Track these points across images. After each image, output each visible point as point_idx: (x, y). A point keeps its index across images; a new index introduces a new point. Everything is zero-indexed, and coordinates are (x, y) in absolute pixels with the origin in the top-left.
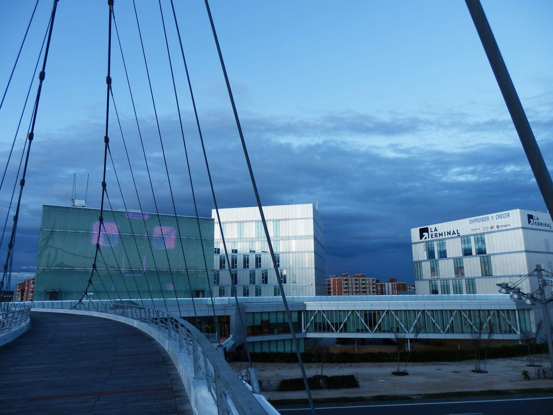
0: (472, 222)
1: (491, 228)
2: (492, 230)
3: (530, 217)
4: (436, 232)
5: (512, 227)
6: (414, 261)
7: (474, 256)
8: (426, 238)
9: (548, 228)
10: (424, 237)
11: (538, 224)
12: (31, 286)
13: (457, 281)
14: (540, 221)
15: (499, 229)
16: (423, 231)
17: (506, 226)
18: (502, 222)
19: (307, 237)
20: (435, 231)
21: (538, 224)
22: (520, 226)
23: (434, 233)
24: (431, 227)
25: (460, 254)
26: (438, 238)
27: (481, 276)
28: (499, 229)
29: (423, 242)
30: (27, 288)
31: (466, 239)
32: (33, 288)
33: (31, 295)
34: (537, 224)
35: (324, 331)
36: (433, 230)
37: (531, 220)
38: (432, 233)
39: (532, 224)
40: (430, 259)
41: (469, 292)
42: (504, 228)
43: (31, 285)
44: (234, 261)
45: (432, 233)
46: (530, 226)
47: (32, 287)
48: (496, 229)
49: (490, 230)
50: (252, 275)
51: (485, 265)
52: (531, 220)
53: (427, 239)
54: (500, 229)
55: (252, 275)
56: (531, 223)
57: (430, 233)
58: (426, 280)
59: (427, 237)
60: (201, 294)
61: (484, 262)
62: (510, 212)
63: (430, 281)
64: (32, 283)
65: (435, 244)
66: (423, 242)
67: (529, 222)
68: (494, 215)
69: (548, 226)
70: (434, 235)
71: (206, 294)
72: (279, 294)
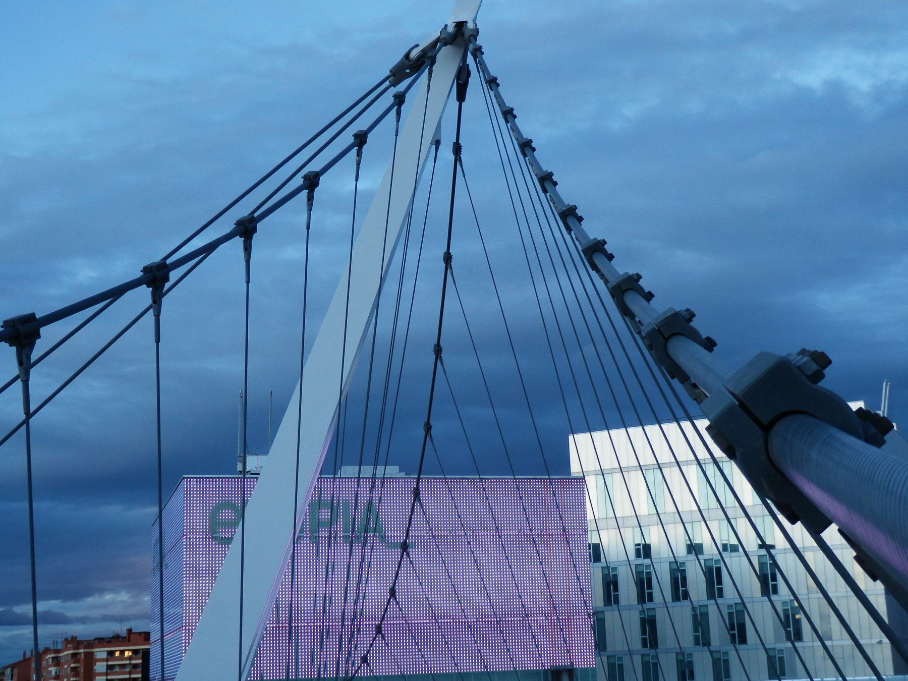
12: (51, 671)
43: (50, 669)
44: (644, 583)
47: (53, 673)
50: (700, 621)
55: (700, 621)
64: (53, 661)
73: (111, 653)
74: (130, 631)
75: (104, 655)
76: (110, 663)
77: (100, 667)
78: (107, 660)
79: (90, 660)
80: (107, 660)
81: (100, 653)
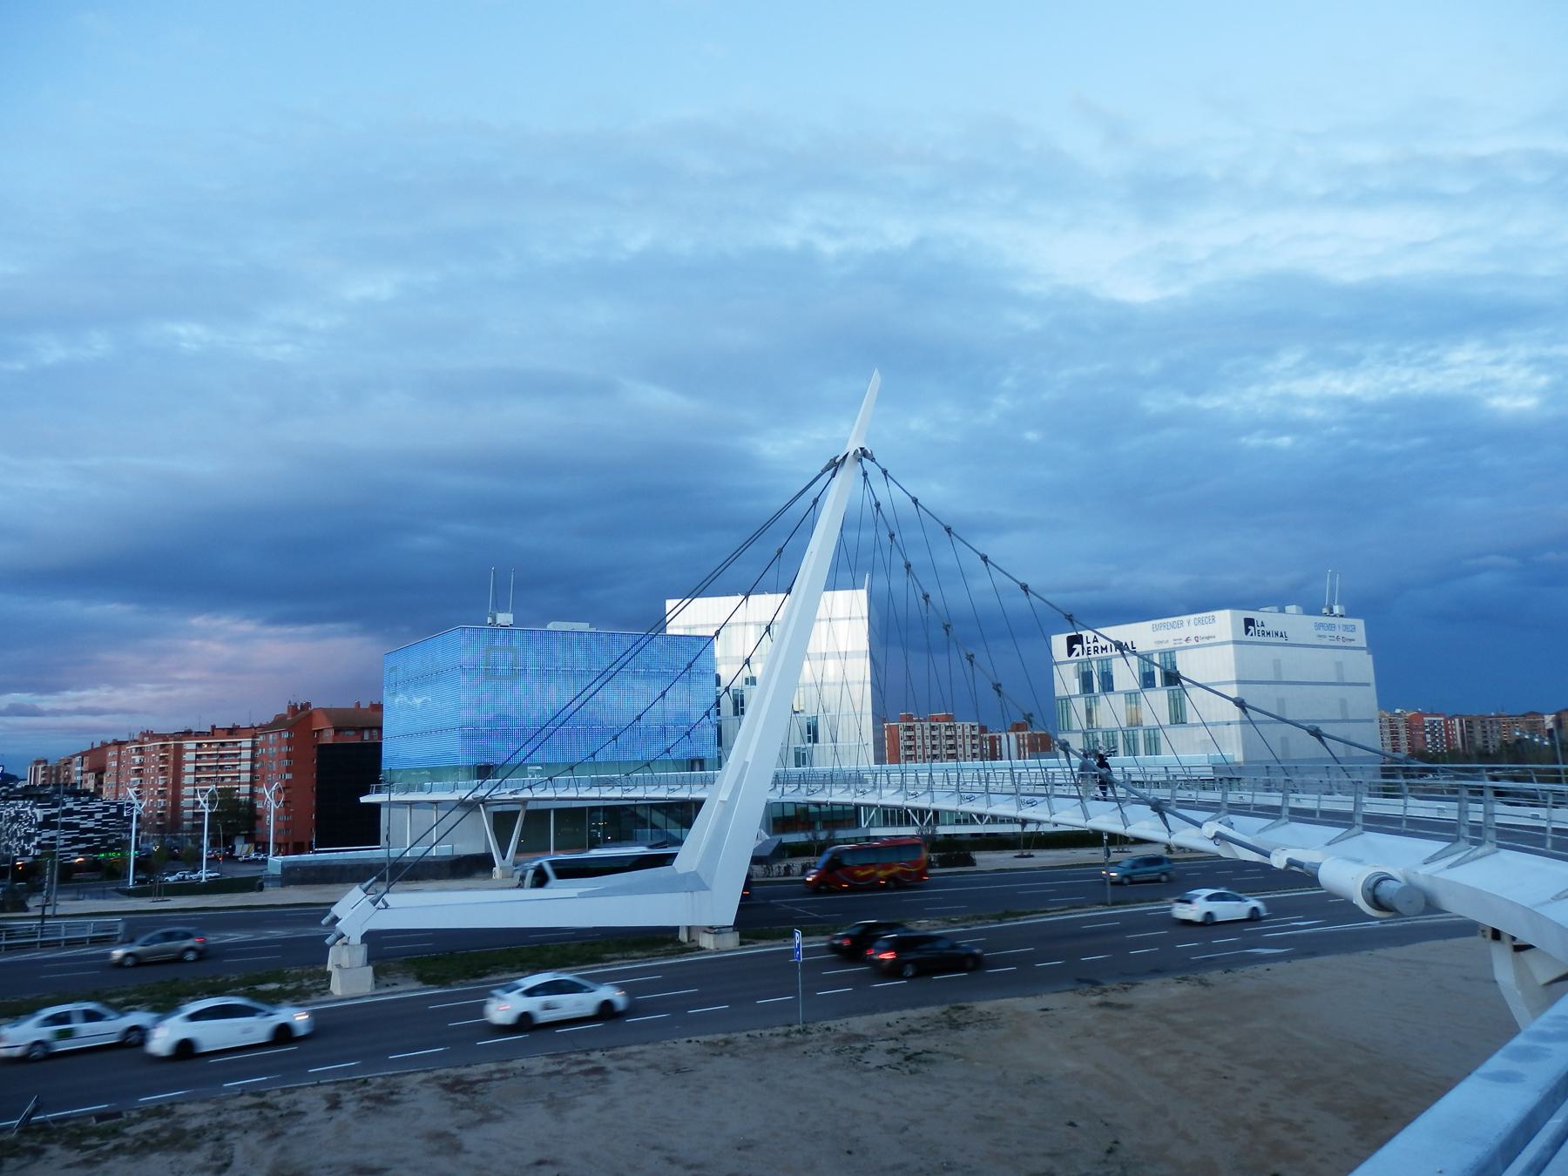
0: (1155, 629)
1: (1187, 640)
2: (1188, 644)
3: (1249, 622)
4: (1096, 644)
5: (1218, 640)
6: (1056, 695)
7: (1159, 689)
8: (1078, 655)
9: (1282, 640)
10: (1075, 653)
11: (1263, 634)
12: (134, 759)
13: (1130, 733)
14: (1266, 629)
15: (1199, 643)
16: (1074, 641)
17: (1208, 638)
18: (1202, 630)
19: (856, 654)
20: (1094, 641)
21: (1263, 634)
22: (1230, 638)
23: (1092, 645)
24: (1087, 634)
25: (1134, 685)
26: (1100, 655)
27: (1169, 723)
28: (1199, 643)
29: (1072, 662)
30: (114, 764)
31: (1145, 658)
32: (141, 764)
33: (135, 781)
34: (1261, 634)
35: (900, 824)
36: (1091, 640)
37: (1250, 627)
38: (1089, 645)
39: (1252, 635)
40: (1084, 693)
41: (1148, 752)
42: (1207, 642)
43: (133, 757)
45: (1089, 645)
46: (1248, 638)
47: (137, 761)
48: (1193, 642)
49: (1185, 644)
51: (1176, 705)
52: (1250, 627)
53: (1081, 657)
54: (1201, 642)
56: (1250, 633)
57: (1086, 646)
58: (1077, 732)
59: (1081, 654)
60: (697, 766)
61: (1175, 700)
62: (1217, 614)
63: (1085, 734)
64: (136, 751)
65: (1094, 664)
66: (1072, 662)
67: (1247, 631)
68: (1192, 617)
69: (1282, 636)
70: (1092, 649)
71: (707, 764)
72: (804, 763)
73: (199, 745)
74: (213, 727)
75: (194, 747)
76: (198, 753)
77: (190, 756)
78: (196, 750)
79: (179, 750)
80: (196, 750)
81: (190, 745)
